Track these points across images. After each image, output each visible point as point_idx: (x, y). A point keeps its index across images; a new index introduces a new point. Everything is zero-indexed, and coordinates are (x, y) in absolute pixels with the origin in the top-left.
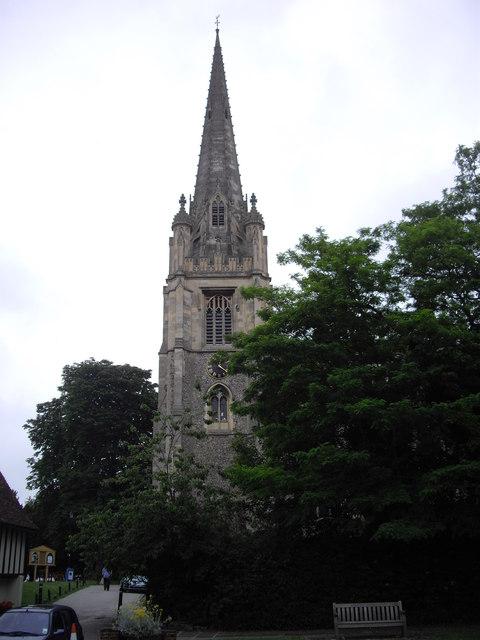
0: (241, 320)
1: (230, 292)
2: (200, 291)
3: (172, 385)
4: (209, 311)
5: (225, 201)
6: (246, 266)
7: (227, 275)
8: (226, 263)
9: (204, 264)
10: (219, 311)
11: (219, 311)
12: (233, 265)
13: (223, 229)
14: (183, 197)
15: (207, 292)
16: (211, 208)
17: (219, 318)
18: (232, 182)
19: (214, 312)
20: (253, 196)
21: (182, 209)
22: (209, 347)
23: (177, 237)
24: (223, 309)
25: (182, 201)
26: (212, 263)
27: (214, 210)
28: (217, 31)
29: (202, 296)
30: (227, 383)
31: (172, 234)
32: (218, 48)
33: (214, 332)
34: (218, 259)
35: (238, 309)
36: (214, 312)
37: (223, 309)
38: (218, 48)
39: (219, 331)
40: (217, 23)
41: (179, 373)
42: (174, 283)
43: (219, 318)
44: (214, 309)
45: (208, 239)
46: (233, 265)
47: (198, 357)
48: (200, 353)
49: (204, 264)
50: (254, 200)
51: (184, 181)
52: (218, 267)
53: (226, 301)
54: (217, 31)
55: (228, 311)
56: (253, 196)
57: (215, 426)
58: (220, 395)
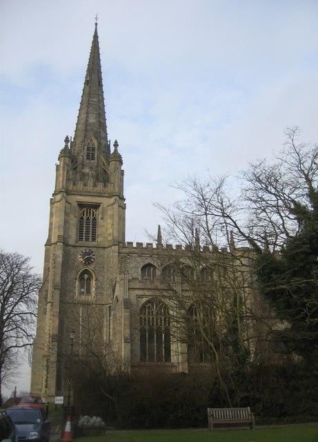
0: (103, 226)
1: (97, 206)
2: (76, 204)
3: (54, 267)
5: (96, 144)
6: (110, 189)
7: (96, 194)
8: (95, 186)
9: (80, 186)
10: (88, 219)
11: (88, 219)
12: (100, 187)
13: (94, 162)
14: (67, 138)
15: (81, 205)
16: (86, 147)
17: (88, 223)
18: (101, 131)
19: (85, 219)
20: (116, 142)
21: (66, 146)
22: (80, 243)
23: (62, 165)
25: (67, 140)
26: (85, 185)
27: (88, 149)
28: (96, 24)
31: (58, 163)
32: (96, 37)
33: (84, 233)
34: (91, 182)
35: (102, 218)
36: (85, 219)
38: (96, 37)
39: (87, 233)
40: (96, 19)
41: (60, 260)
42: (59, 197)
43: (88, 223)
44: (85, 217)
45: (83, 168)
46: (100, 187)
47: (73, 250)
48: (74, 246)
49: (80, 186)
50: (116, 145)
51: (65, 124)
52: (90, 188)
54: (96, 24)
55: (94, 219)
56: (116, 142)
57: (83, 298)
58: (86, 276)
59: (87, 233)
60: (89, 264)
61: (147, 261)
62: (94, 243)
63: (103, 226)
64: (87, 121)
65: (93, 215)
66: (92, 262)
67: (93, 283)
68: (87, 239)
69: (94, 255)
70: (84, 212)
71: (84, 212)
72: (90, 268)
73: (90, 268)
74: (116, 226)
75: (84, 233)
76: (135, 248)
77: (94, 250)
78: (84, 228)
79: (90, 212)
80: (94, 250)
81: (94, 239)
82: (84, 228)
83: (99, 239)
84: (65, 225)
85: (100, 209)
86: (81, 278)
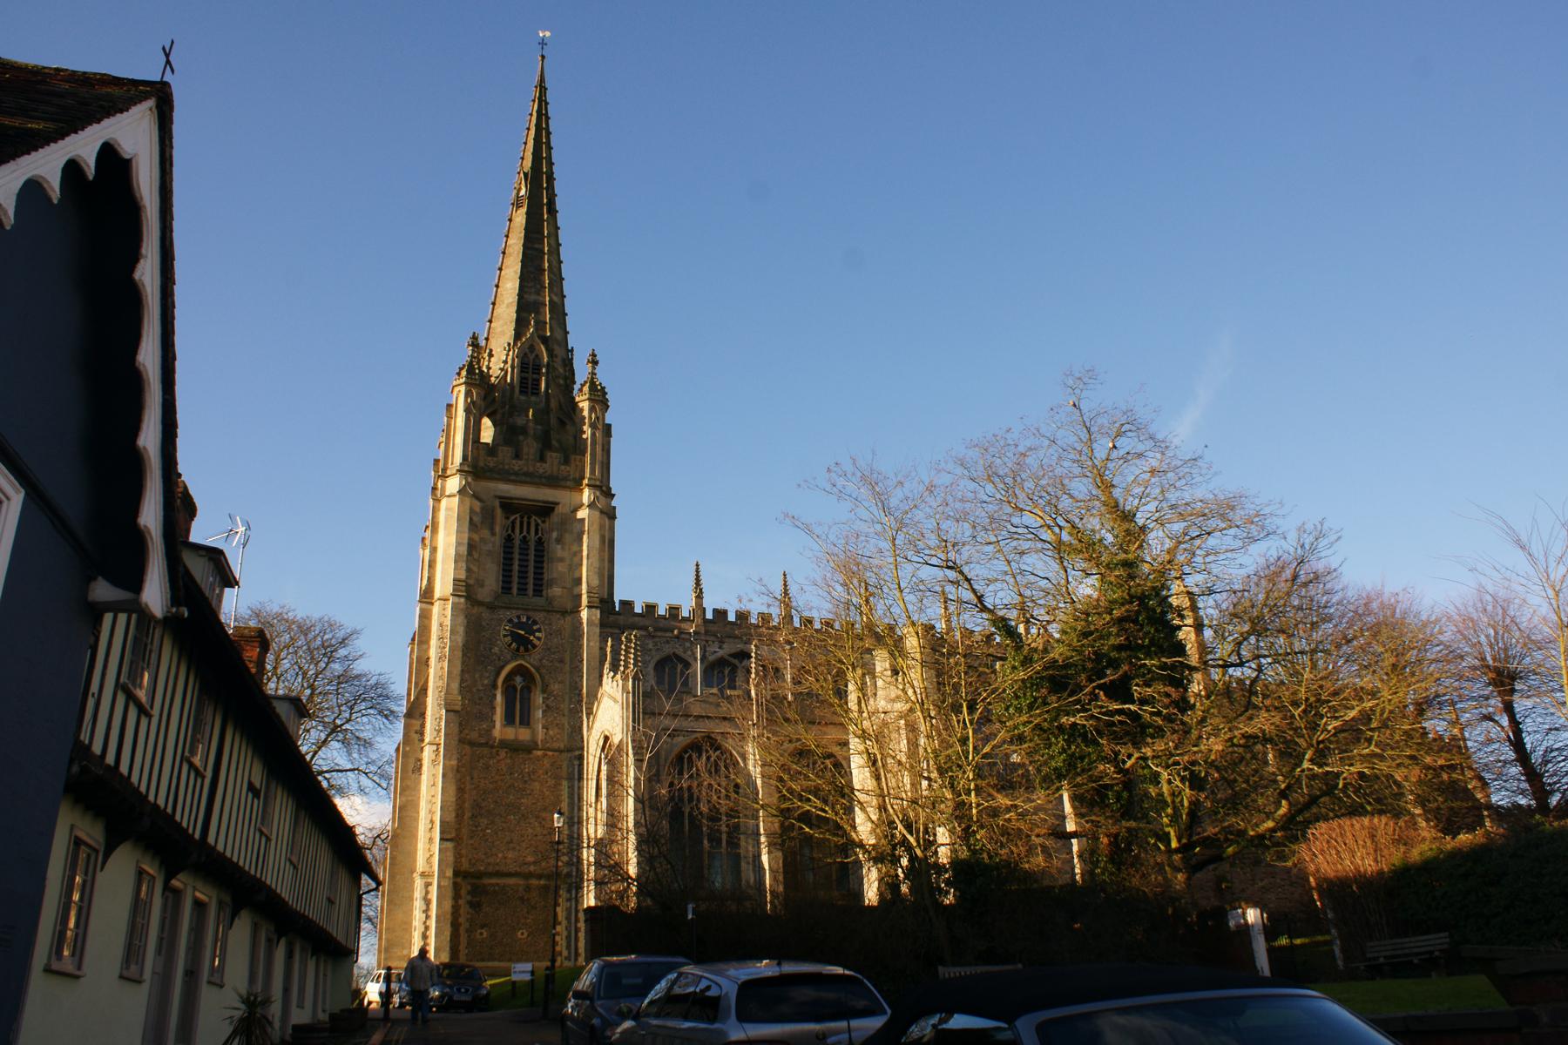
0: (562, 560)
1: (547, 510)
2: (497, 503)
4: (509, 539)
8: (542, 459)
10: (524, 540)
11: (524, 540)
15: (509, 506)
19: (517, 542)
24: (532, 537)
29: (499, 511)
35: (558, 541)
36: (517, 542)
37: (532, 537)
38: (542, 87)
39: (523, 574)
53: (537, 525)
54: (543, 57)
55: (540, 542)
59: (523, 574)
61: (668, 650)
62: (539, 601)
63: (562, 560)
65: (536, 533)
67: (538, 698)
68: (522, 590)
70: (513, 523)
71: (513, 523)
76: (638, 615)
77: (539, 616)
78: (516, 563)
79: (529, 524)
80: (539, 616)
81: (538, 592)
82: (516, 563)
84: (470, 553)
85: (555, 518)
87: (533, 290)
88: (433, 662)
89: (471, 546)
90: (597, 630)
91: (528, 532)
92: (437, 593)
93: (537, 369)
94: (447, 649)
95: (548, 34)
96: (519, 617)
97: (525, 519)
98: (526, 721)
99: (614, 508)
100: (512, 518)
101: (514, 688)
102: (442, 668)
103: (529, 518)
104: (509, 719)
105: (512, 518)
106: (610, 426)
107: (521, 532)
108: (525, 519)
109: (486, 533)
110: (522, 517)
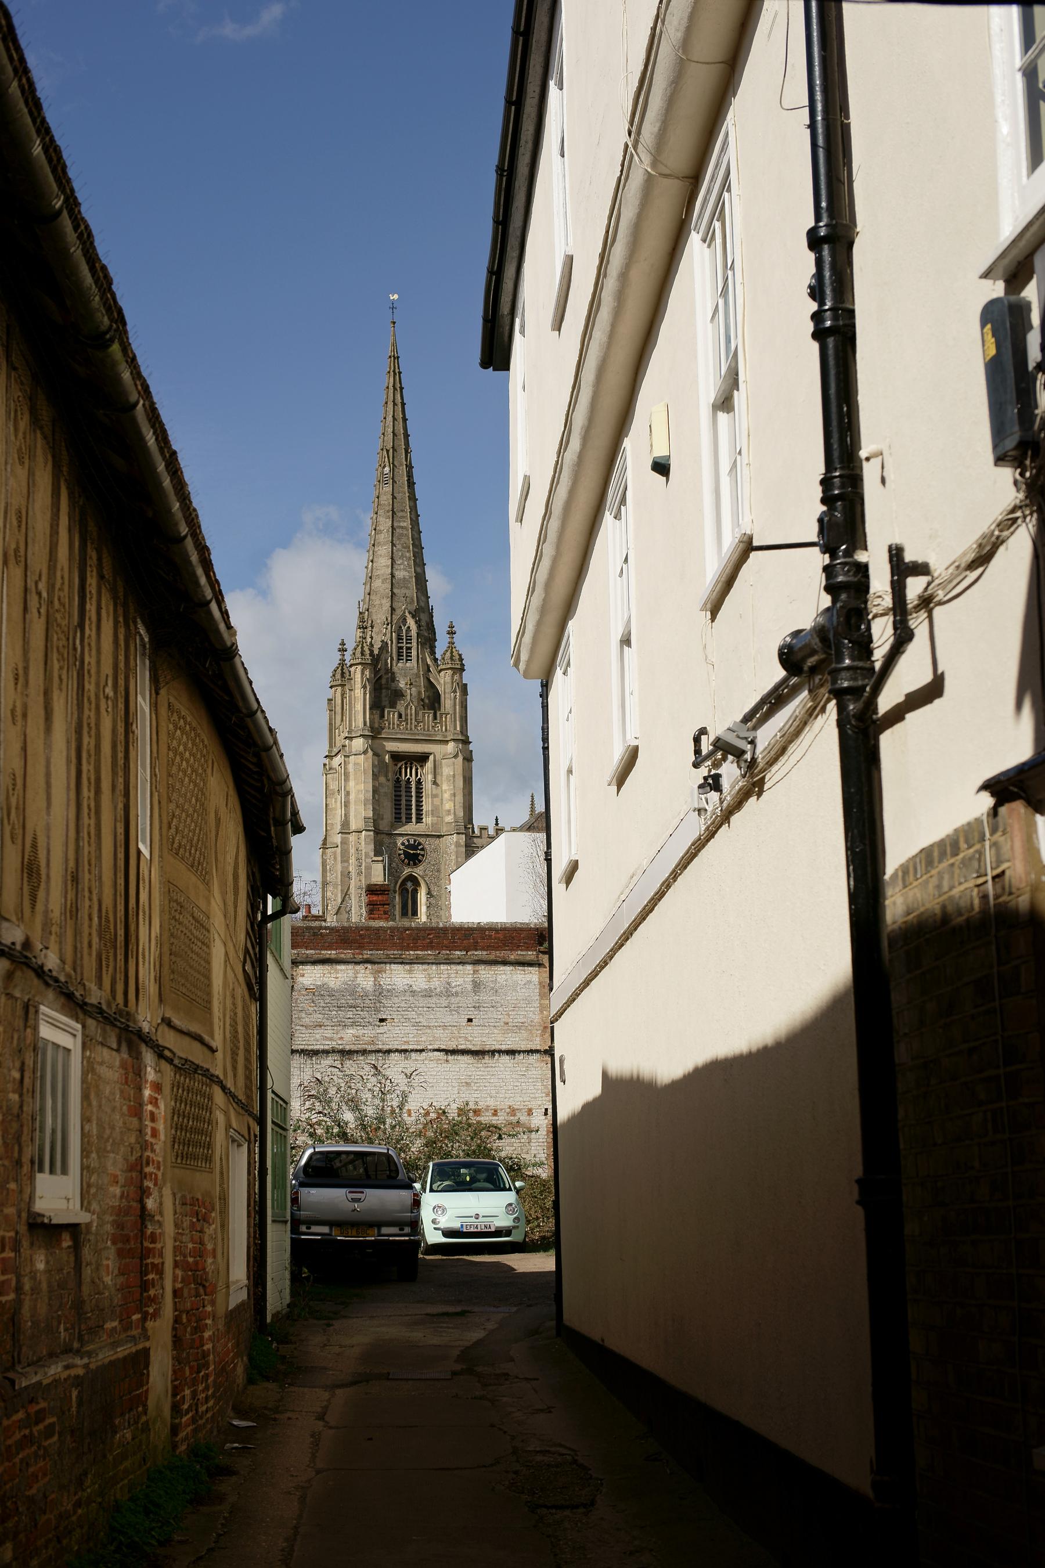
15: (396, 757)
30: (421, 873)
55: (419, 782)
58: (409, 885)
60: (415, 864)
64: (393, 576)
65: (417, 775)
66: (420, 861)
69: (422, 849)
70: (400, 768)
72: (418, 871)
73: (418, 871)
74: (460, 798)
75: (403, 807)
77: (422, 840)
80: (422, 840)
81: (419, 820)
83: (428, 820)
84: (374, 797)
85: (429, 764)
86: (404, 891)
87: (402, 567)
88: (353, 875)
89: (375, 791)
90: (464, 849)
91: (411, 775)
92: (353, 826)
93: (409, 640)
94: (363, 867)
95: (396, 297)
96: (408, 841)
97: (408, 765)
98: (415, 913)
99: (471, 751)
100: (399, 765)
101: (407, 890)
102: (360, 881)
103: (411, 764)
104: (404, 913)
105: (399, 765)
106: (466, 685)
107: (406, 775)
108: (408, 765)
109: (382, 779)
110: (406, 764)
